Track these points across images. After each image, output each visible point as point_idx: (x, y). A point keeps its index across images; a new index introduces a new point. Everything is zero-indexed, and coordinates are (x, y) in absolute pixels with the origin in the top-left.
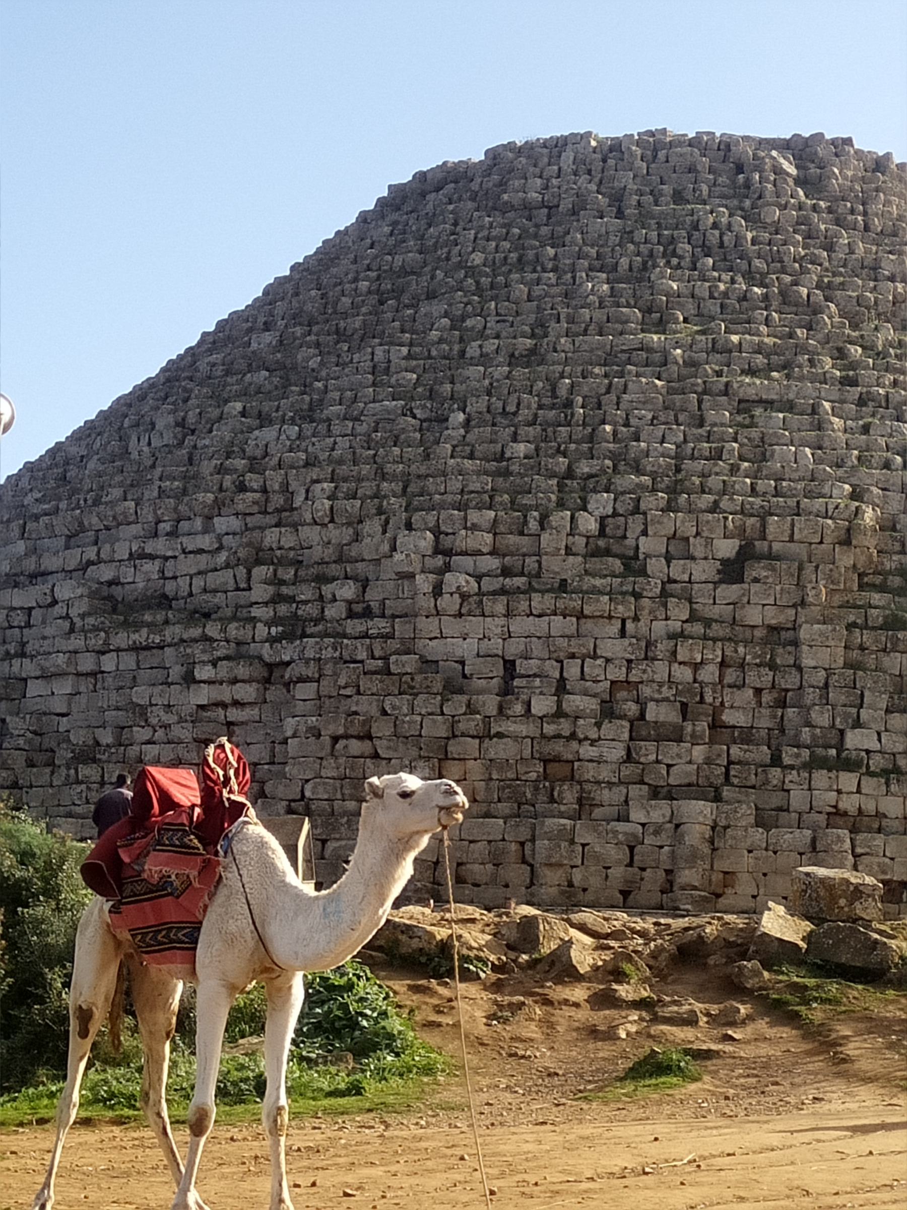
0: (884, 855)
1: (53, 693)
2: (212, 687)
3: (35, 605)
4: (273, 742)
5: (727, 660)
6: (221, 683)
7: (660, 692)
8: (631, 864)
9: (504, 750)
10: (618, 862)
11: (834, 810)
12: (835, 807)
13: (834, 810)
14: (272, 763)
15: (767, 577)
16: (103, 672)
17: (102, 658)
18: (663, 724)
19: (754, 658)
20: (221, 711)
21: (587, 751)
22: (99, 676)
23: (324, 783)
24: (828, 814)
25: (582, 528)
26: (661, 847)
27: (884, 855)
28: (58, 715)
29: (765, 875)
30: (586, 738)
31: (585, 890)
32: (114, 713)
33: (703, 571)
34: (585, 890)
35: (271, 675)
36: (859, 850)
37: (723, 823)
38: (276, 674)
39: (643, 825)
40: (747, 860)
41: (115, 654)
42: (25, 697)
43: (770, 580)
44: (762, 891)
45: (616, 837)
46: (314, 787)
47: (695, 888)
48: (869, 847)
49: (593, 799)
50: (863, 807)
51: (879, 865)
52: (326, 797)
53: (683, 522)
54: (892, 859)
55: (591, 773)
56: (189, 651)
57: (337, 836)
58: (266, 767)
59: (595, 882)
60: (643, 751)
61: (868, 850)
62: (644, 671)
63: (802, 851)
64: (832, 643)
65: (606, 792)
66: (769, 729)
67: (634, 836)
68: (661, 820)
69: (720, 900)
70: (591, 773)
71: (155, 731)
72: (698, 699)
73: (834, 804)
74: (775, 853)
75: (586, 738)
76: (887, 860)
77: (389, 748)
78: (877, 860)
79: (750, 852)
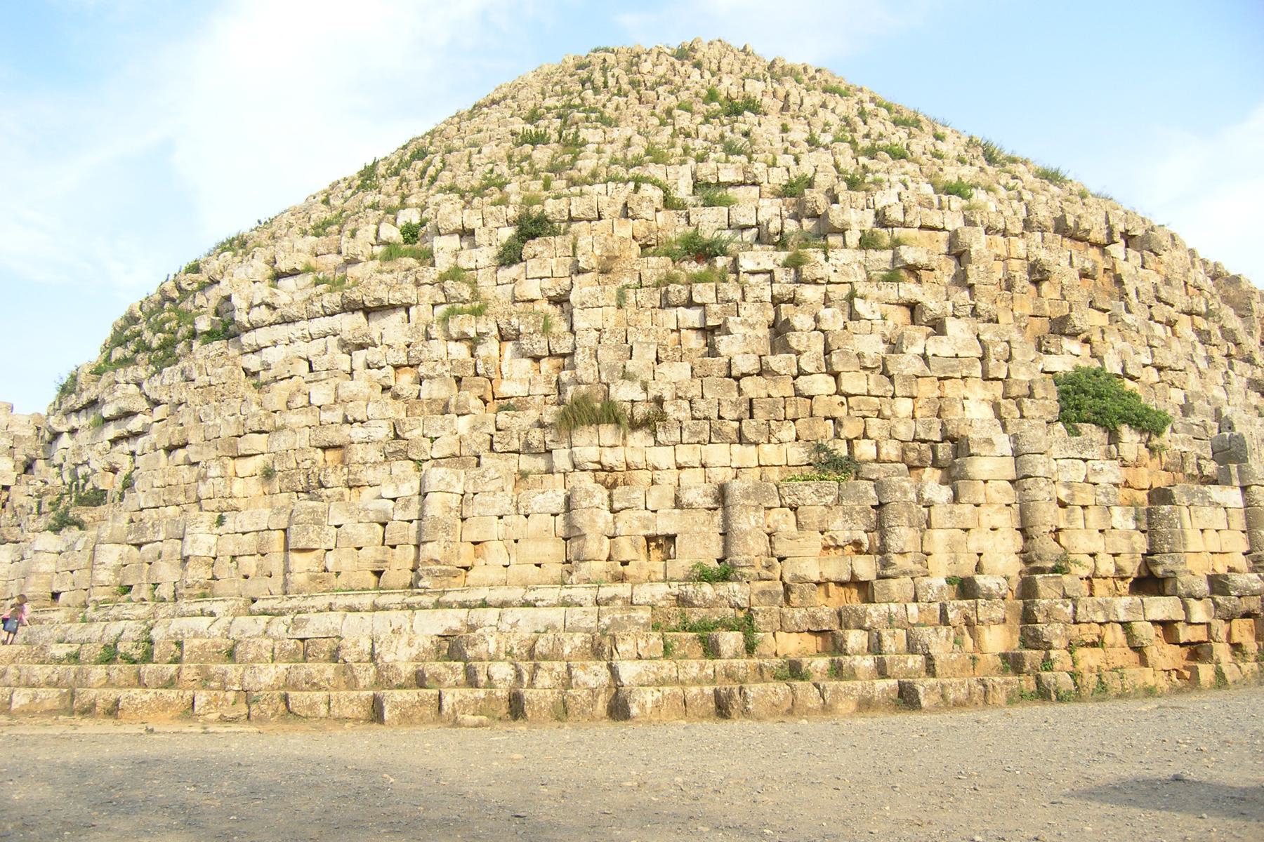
0: (646, 509)
5: (504, 333)
7: (434, 369)
8: (383, 544)
9: (284, 441)
10: (370, 542)
11: (599, 467)
12: (599, 463)
13: (599, 467)
15: (542, 252)
18: (435, 400)
19: (527, 327)
21: (357, 432)
24: (595, 471)
25: (383, 236)
26: (411, 521)
27: (646, 509)
29: (516, 541)
30: (355, 421)
31: (338, 574)
33: (485, 256)
34: (338, 574)
36: (617, 506)
37: (471, 489)
39: (394, 500)
40: (497, 528)
43: (546, 254)
44: (513, 561)
45: (366, 515)
47: (437, 562)
48: (628, 500)
49: (360, 480)
50: (629, 460)
51: (639, 519)
53: (469, 216)
54: (655, 511)
55: (360, 455)
59: (347, 564)
60: (407, 427)
61: (627, 505)
62: (421, 352)
63: (555, 511)
64: (602, 303)
65: (371, 471)
66: (546, 396)
67: (386, 513)
68: (409, 493)
69: (470, 573)
70: (360, 455)
72: (471, 372)
73: (597, 459)
74: (527, 516)
75: (355, 421)
76: (648, 513)
77: (196, 452)
78: (637, 514)
79: (500, 517)
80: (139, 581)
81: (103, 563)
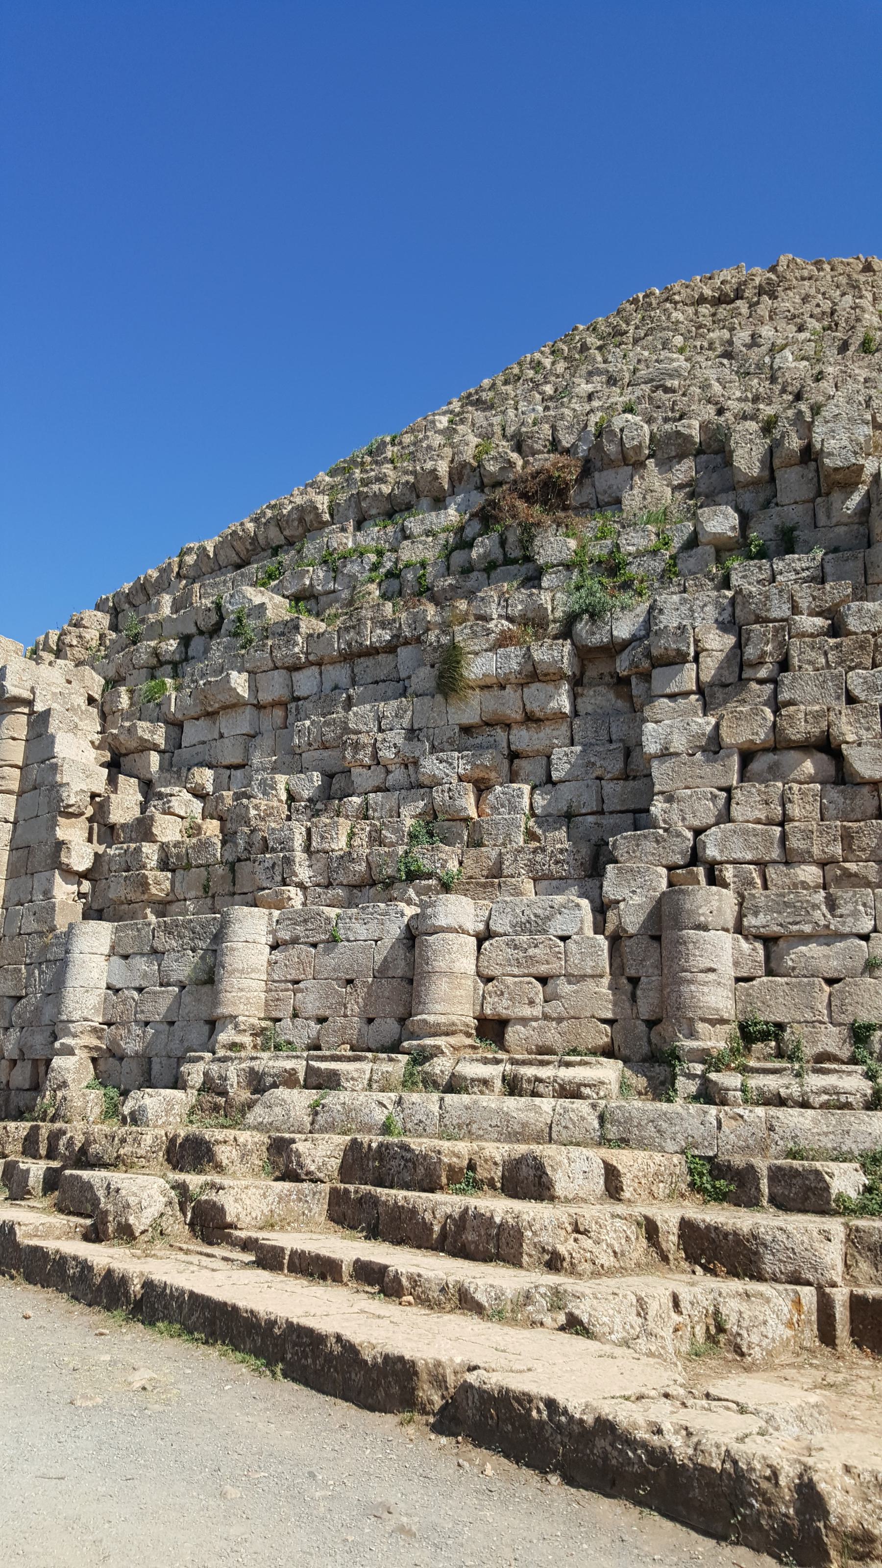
1: (222, 736)
2: (486, 692)
3: (193, 630)
4: (600, 778)
6: (502, 687)
14: (602, 812)
16: (298, 699)
17: (296, 676)
20: (500, 734)
22: (293, 705)
23: (746, 832)
28: (228, 767)
32: (316, 754)
35: (582, 674)
38: (592, 672)
41: (315, 669)
42: (180, 747)
46: (725, 839)
52: (749, 857)
56: (445, 640)
57: (807, 929)
58: (590, 819)
71: (388, 772)
80: (809, 1016)
81: (712, 970)
